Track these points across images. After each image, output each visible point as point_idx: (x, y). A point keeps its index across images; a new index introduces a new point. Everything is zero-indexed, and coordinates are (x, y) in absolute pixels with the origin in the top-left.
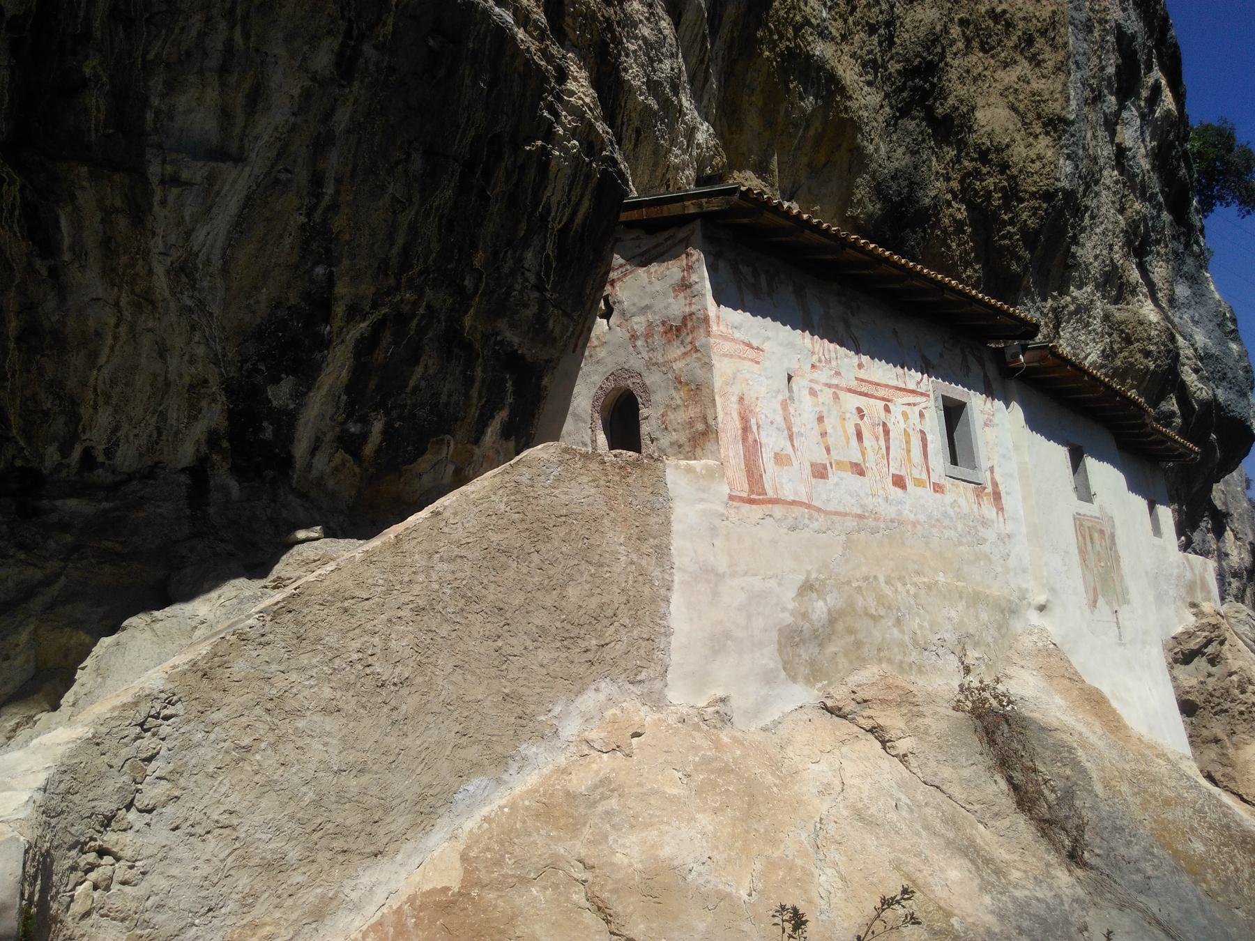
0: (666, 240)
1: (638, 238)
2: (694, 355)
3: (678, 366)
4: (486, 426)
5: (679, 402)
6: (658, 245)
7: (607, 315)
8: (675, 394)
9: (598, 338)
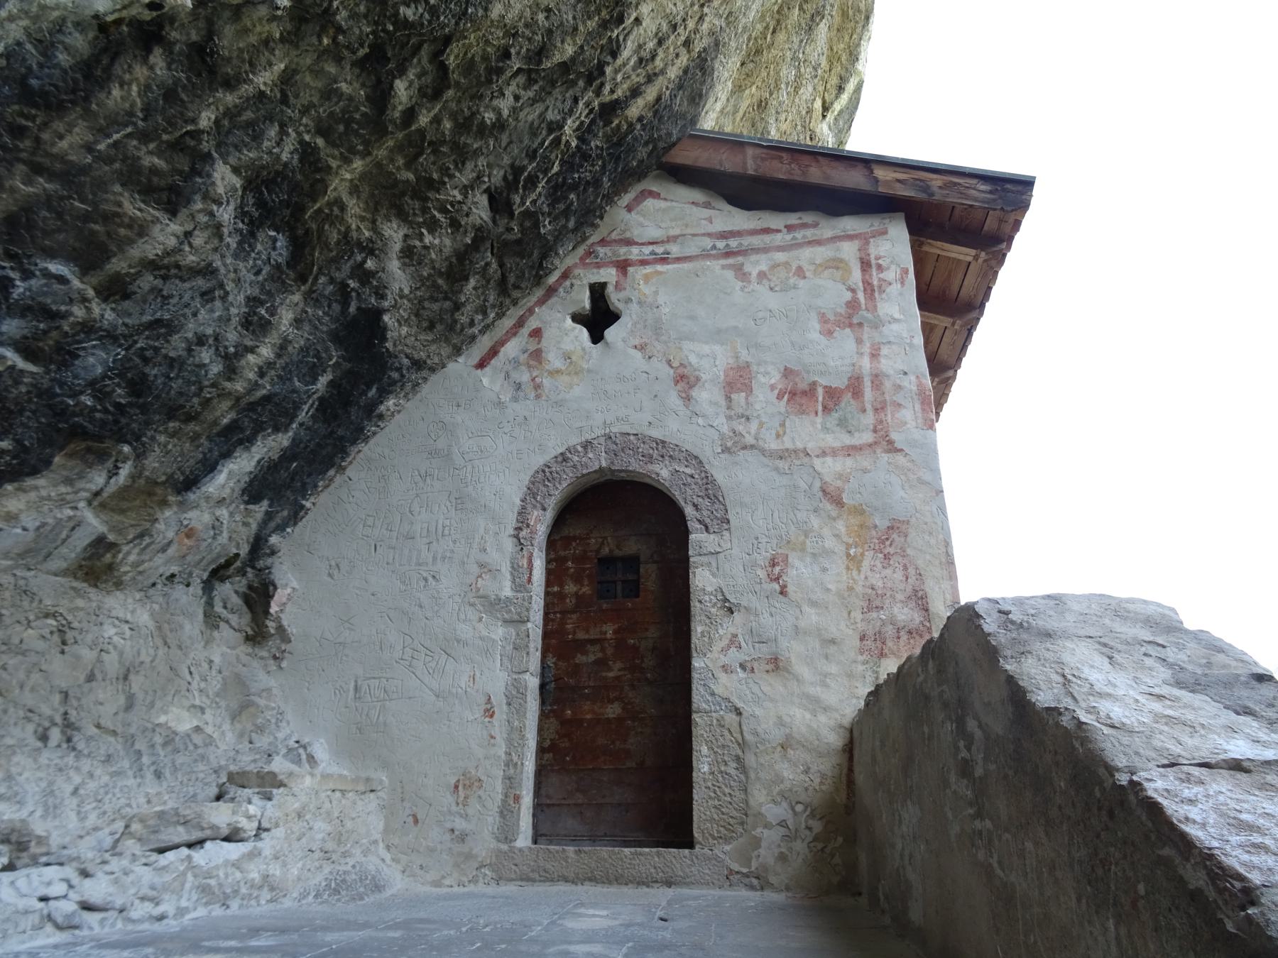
0: (790, 228)
1: (707, 205)
2: (885, 457)
3: (830, 467)
4: (227, 455)
5: (830, 543)
6: (767, 231)
7: (599, 318)
8: (815, 522)
9: (567, 357)
